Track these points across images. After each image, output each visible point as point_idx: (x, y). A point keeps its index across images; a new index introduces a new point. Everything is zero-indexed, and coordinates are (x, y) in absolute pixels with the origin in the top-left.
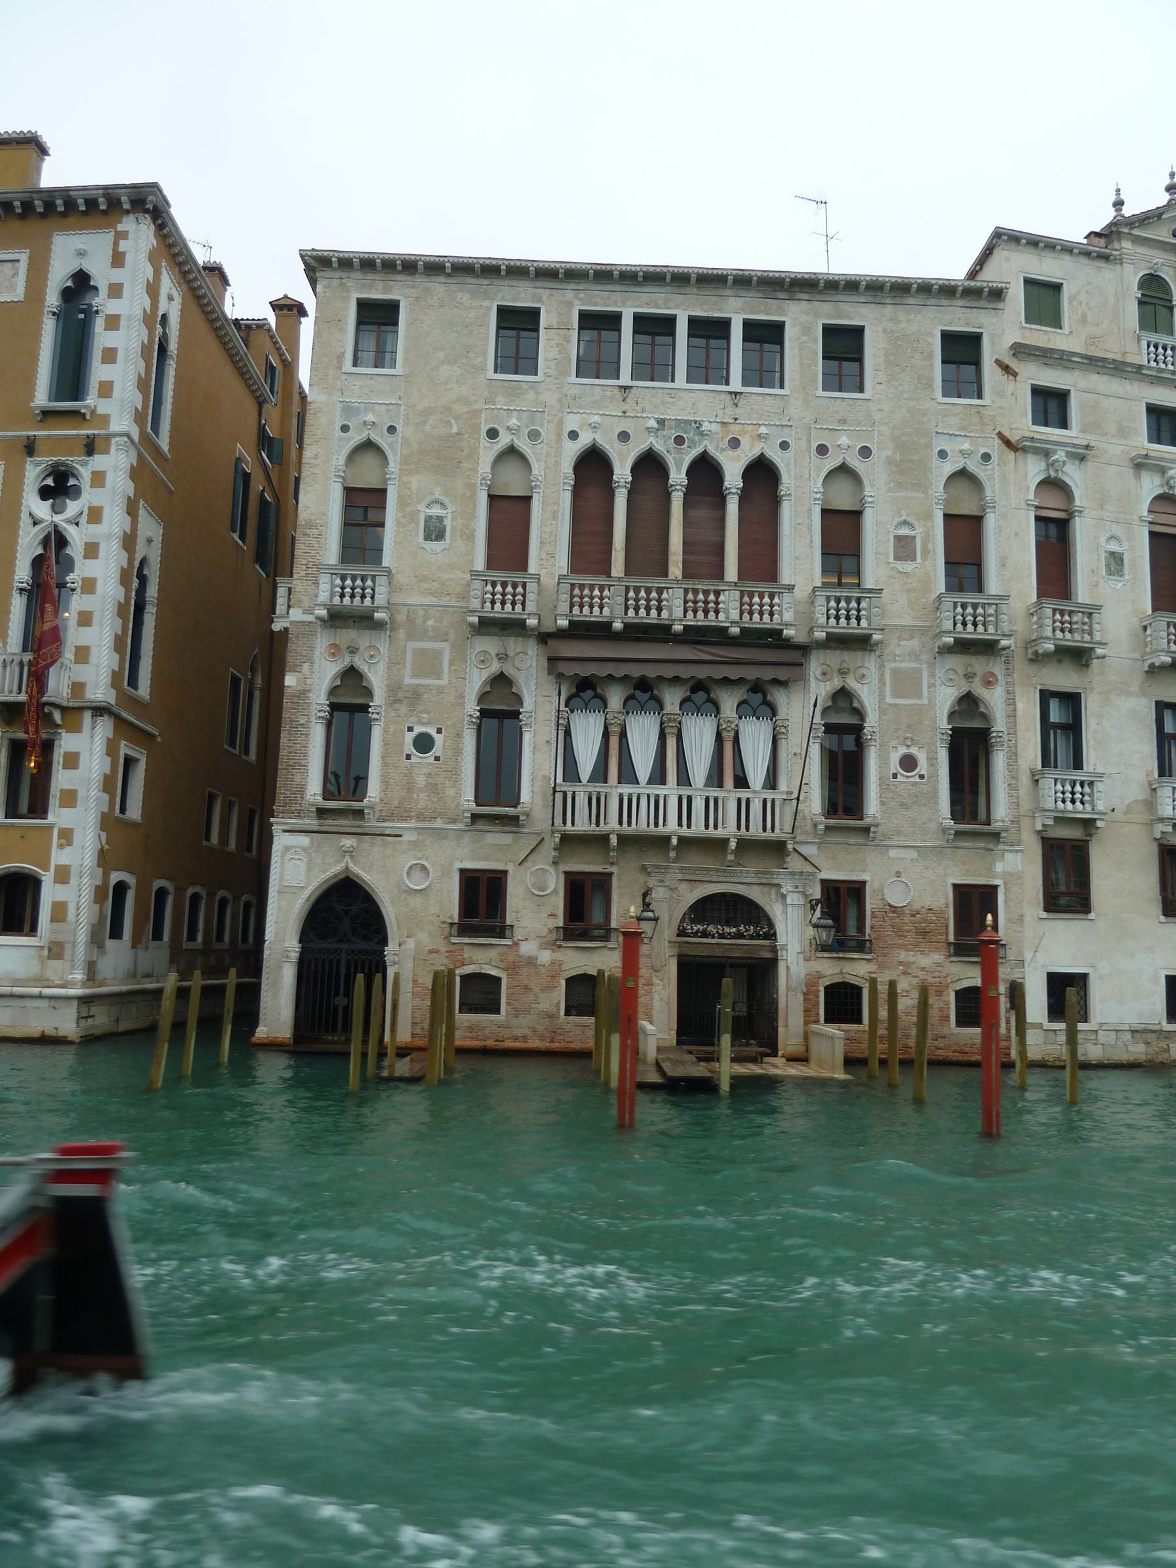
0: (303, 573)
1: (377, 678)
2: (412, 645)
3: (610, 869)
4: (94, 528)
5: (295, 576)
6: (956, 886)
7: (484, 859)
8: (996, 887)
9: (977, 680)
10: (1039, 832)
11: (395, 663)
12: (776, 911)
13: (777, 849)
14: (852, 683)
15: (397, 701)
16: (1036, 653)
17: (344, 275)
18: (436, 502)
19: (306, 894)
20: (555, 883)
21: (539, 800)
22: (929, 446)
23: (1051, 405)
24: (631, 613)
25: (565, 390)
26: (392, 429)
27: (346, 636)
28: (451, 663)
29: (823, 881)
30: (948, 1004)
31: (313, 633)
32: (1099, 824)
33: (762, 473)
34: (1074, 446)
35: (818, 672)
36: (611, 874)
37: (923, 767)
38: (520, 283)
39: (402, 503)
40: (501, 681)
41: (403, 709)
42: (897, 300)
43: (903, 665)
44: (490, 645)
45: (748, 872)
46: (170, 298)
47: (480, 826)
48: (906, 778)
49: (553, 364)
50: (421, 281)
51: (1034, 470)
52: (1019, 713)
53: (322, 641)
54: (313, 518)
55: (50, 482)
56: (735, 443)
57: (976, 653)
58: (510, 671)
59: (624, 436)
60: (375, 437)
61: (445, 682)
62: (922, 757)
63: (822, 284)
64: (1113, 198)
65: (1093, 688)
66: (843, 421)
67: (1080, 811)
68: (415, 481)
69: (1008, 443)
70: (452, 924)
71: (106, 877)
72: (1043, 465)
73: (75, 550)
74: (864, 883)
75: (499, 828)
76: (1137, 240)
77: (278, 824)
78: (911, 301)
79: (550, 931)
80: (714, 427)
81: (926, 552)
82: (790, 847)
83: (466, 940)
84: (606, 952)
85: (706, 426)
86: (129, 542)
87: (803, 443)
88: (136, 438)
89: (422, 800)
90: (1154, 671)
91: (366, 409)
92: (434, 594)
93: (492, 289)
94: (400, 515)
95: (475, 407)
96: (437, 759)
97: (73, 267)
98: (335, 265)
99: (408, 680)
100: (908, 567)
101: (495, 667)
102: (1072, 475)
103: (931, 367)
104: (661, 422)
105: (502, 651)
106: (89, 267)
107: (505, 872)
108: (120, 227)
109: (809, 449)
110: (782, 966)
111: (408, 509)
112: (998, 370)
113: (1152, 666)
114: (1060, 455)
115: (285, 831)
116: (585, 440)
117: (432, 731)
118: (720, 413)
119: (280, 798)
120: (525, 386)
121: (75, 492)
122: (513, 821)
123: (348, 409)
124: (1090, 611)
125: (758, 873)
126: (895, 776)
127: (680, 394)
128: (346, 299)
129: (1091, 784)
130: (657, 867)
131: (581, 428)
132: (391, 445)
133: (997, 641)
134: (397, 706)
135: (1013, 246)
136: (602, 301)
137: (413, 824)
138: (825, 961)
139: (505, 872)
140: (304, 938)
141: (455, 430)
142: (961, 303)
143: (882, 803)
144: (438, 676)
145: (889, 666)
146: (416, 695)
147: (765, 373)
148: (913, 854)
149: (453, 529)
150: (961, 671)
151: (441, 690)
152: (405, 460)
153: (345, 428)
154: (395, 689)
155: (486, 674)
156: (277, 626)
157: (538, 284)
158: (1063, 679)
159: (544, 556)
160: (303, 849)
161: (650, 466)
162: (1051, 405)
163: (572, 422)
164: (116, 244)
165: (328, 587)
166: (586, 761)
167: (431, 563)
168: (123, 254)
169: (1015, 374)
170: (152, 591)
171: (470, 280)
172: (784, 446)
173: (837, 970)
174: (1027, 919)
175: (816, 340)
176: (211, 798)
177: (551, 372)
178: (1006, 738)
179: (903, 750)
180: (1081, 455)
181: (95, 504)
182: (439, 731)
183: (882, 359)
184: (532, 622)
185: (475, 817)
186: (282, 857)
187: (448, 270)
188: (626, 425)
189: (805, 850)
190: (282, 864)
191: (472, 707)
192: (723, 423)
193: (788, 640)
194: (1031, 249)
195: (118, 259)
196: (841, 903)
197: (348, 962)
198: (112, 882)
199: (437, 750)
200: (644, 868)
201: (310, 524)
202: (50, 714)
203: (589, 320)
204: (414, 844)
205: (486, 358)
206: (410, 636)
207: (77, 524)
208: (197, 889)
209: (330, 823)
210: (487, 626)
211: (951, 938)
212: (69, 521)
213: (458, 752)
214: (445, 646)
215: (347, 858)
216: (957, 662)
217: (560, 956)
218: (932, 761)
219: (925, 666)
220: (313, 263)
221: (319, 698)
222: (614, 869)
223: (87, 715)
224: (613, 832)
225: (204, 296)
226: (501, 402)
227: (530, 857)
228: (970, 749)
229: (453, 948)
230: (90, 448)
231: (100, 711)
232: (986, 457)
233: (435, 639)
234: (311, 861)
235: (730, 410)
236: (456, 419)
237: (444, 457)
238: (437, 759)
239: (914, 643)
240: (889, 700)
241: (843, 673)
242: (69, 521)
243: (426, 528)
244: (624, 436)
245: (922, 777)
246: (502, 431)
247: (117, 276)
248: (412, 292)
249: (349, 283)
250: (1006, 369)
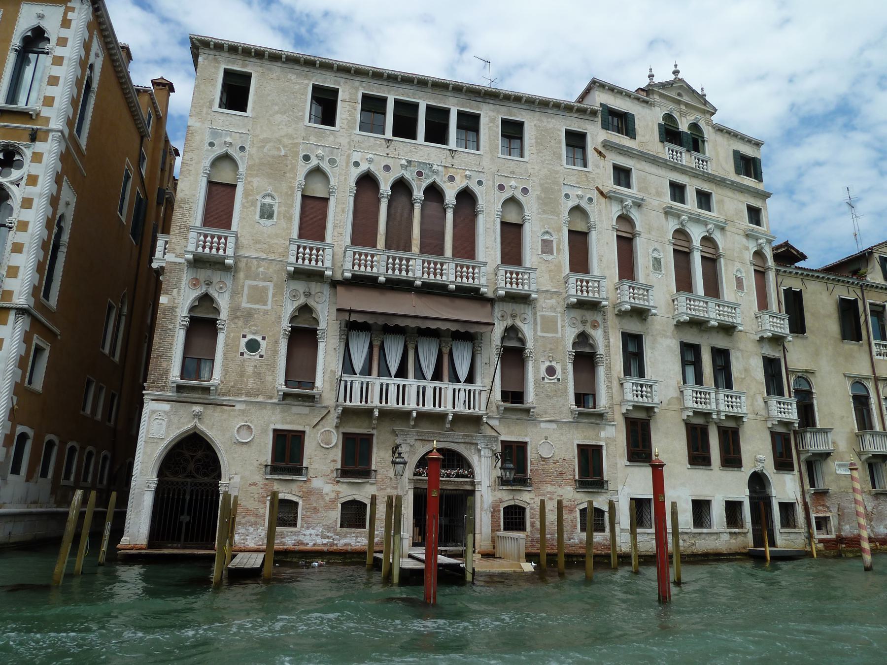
0: (177, 231)
1: (223, 302)
2: (248, 283)
3: (372, 432)
4: (30, 189)
5: (172, 233)
6: (578, 445)
8: (601, 446)
9: (588, 324)
10: (624, 414)
11: (235, 293)
12: (474, 459)
13: (475, 421)
14: (519, 323)
15: (237, 318)
16: (620, 311)
17: (217, 53)
18: (269, 195)
19: (166, 442)
20: (336, 439)
21: (327, 386)
22: (560, 191)
23: (622, 175)
24: (390, 272)
25: (352, 137)
26: (242, 148)
27: (203, 274)
28: (274, 296)
29: (502, 442)
30: (575, 518)
31: (182, 270)
32: (656, 410)
33: (466, 197)
34: (636, 198)
35: (499, 315)
36: (372, 435)
37: (559, 374)
38: (328, 73)
39: (247, 194)
40: (305, 310)
42: (542, 110)
43: (547, 314)
44: (300, 286)
45: (458, 435)
46: (97, 55)
47: (289, 401)
48: (548, 380)
49: (345, 122)
50: (267, 64)
51: (615, 210)
52: (611, 344)
53: (186, 277)
54: (187, 197)
56: (452, 179)
57: (588, 309)
58: (312, 303)
59: (387, 168)
60: (231, 151)
61: (269, 307)
62: (558, 368)
63: (502, 96)
64: (648, 73)
65: (648, 333)
67: (644, 401)
68: (256, 182)
69: (602, 193)
70: (266, 466)
71: (13, 429)
72: (620, 208)
74: (526, 443)
75: (301, 403)
76: (662, 96)
77: (148, 394)
78: (549, 111)
79: (332, 472)
80: (440, 168)
81: (559, 250)
82: (485, 420)
83: (276, 477)
84: (368, 486)
85: (435, 167)
86: (54, 201)
87: (491, 183)
88: (67, 136)
89: (250, 383)
90: (680, 325)
91: (226, 134)
92: (264, 251)
93: (310, 74)
94: (244, 201)
95: (296, 141)
97: (34, 23)
98: (212, 47)
99: (245, 305)
100: (549, 257)
101: (302, 301)
102: (635, 214)
103: (560, 148)
104: (409, 162)
105: (307, 290)
106: (44, 24)
107: (304, 432)
108: (69, 4)
109: (494, 186)
110: (478, 494)
111: (251, 198)
112: (596, 154)
113: (678, 322)
114: (629, 202)
115: (153, 400)
117: (259, 338)
119: (150, 377)
120: (328, 132)
121: (20, 165)
122: (311, 398)
123: (215, 133)
124: (647, 288)
125: (464, 435)
126: (543, 379)
127: (421, 147)
128: (218, 68)
129: (651, 386)
130: (402, 430)
131: (361, 160)
132: (241, 158)
133: (600, 302)
134: (236, 321)
135: (601, 89)
136: (376, 90)
137: (243, 398)
138: (503, 492)
139: (304, 432)
140: (160, 474)
141: (283, 153)
142: (576, 115)
143: (536, 395)
144: (265, 303)
145: (539, 314)
146: (249, 315)
148: (554, 426)
149: (279, 213)
150: (579, 318)
151: (266, 312)
152: (250, 168)
153: (211, 144)
154: (235, 311)
155: (296, 304)
156: (155, 265)
157: (338, 75)
158: (634, 327)
159: (336, 234)
160: (165, 412)
161: (401, 186)
162: (622, 175)
163: (356, 157)
164: (65, 14)
166: (358, 362)
167: (263, 234)
168: (70, 21)
169: (604, 157)
170: (65, 237)
171: (296, 67)
172: (480, 183)
173: (511, 497)
174: (619, 466)
175: (497, 127)
176: (89, 383)
177: (344, 126)
178: (604, 358)
179: (548, 364)
180: (638, 205)
181: (33, 173)
182: (264, 338)
183: (534, 141)
184: (328, 273)
185: (286, 395)
186: (150, 417)
187: (284, 59)
188: (389, 162)
189: (491, 422)
190: (149, 422)
191: (286, 325)
192: (445, 167)
193: (482, 294)
194: (610, 92)
195: (66, 23)
196: (514, 455)
197: (192, 490)
198: (18, 433)
199: (262, 350)
200: (394, 432)
201: (184, 201)
204: (243, 412)
205: (304, 113)
206: (247, 277)
207: (18, 185)
208: (74, 444)
209: (185, 396)
210: (299, 274)
211: (577, 477)
212: (12, 183)
213: (275, 353)
214: (271, 285)
215: (196, 420)
216: (577, 314)
217: (338, 488)
218: (564, 370)
219: (559, 315)
220: (198, 44)
221: (183, 312)
222: (374, 432)
223: (12, 316)
225: (117, 60)
226: (313, 140)
227: (321, 423)
229: (267, 482)
230: (34, 137)
231: (21, 311)
232: (590, 200)
233: (264, 280)
234: (170, 420)
235: (449, 159)
236: (284, 147)
237: (275, 168)
238: (261, 356)
239: (553, 302)
240: (539, 334)
241: (514, 317)
242: (12, 183)
243: (262, 211)
244: (387, 168)
245: (558, 380)
246: (313, 157)
247: (64, 33)
248: (259, 69)
249: (220, 59)
250: (600, 153)
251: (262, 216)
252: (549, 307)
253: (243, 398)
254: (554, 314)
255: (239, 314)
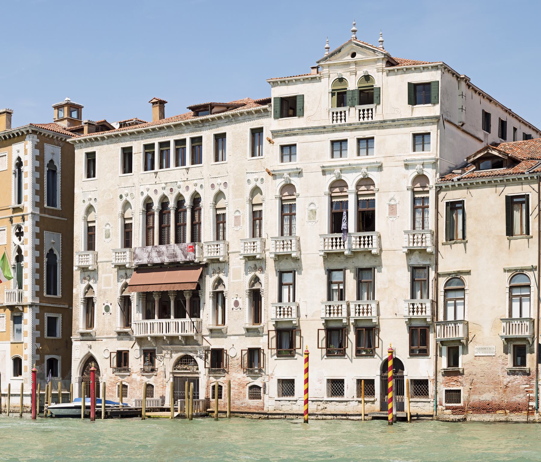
2: (104, 275)
7: (123, 347)
12: (198, 360)
15: (101, 295)
37: (241, 305)
41: (102, 297)
55: (17, 231)
56: (187, 187)
66: (219, 173)
73: (23, 254)
85: (179, 183)
96: (111, 314)
99: (103, 288)
116: (145, 195)
117: (109, 304)
118: (183, 177)
139: (128, 351)
147: (197, 159)
154: (100, 291)
163: (142, 189)
165: (78, 259)
182: (111, 304)
185: (119, 333)
191: (119, 295)
202: (18, 308)
203: (146, 147)
209: (85, 338)
213: (116, 311)
214: (112, 275)
218: (243, 302)
224: (148, 336)
228: (256, 297)
231: (31, 306)
240: (232, 281)
245: (240, 309)
246: (124, 196)
251: (106, 238)
252: (237, 264)
253: (105, 336)
254: (239, 266)
255: (101, 293)
